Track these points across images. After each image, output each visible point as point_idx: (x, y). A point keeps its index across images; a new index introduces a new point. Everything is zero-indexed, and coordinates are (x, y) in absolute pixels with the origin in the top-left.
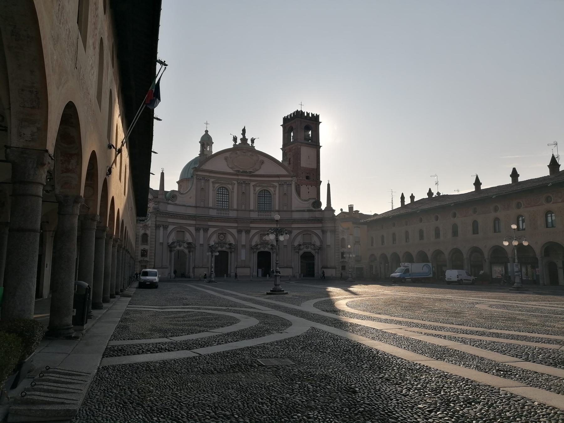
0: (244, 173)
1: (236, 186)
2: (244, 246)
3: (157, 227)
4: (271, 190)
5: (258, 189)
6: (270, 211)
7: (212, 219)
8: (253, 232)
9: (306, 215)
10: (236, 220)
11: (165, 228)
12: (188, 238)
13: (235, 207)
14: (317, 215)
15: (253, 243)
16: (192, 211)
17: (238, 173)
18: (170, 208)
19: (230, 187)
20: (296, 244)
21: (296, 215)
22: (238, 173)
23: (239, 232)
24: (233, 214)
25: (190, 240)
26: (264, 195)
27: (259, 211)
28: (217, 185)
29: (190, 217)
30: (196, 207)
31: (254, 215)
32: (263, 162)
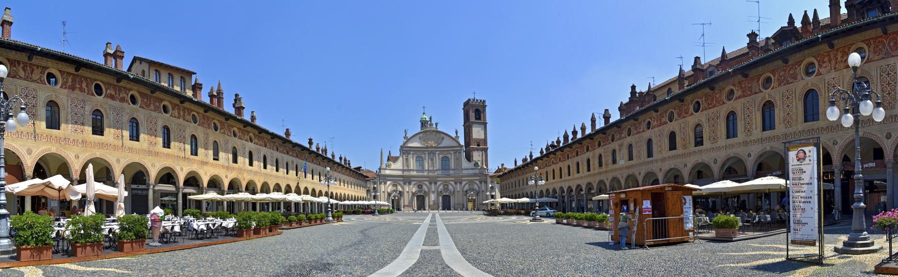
3: (380, 183)
4: (449, 156)
6: (449, 169)
7: (413, 176)
8: (439, 183)
9: (471, 172)
10: (427, 177)
11: (385, 183)
12: (399, 188)
14: (477, 171)
16: (400, 173)
18: (388, 172)
20: (465, 189)
21: (465, 172)
24: (426, 174)
26: (445, 160)
29: (399, 176)
32: (443, 139)
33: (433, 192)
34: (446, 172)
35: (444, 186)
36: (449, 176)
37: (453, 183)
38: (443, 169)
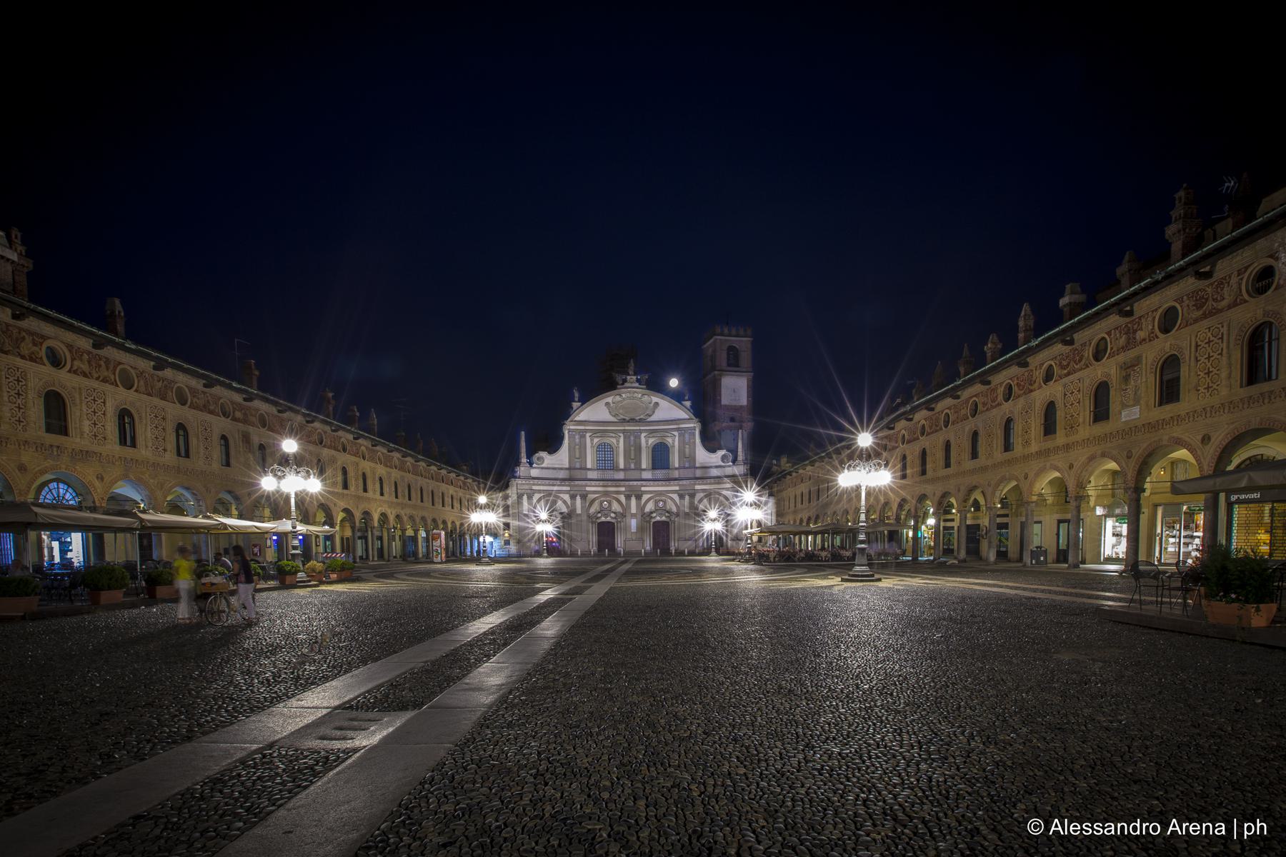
0: (632, 420)
1: (622, 440)
2: (633, 516)
4: (670, 440)
5: (651, 441)
8: (645, 497)
9: (715, 472)
13: (622, 466)
15: (647, 509)
16: (562, 475)
17: (624, 421)
19: (614, 441)
22: (624, 421)
23: (628, 497)
25: (565, 510)
27: (654, 467)
28: (596, 440)
30: (569, 469)
31: (647, 475)
33: (633, 516)
34: (660, 473)
35: (656, 503)
36: (669, 480)
37: (675, 497)
38: (654, 467)
